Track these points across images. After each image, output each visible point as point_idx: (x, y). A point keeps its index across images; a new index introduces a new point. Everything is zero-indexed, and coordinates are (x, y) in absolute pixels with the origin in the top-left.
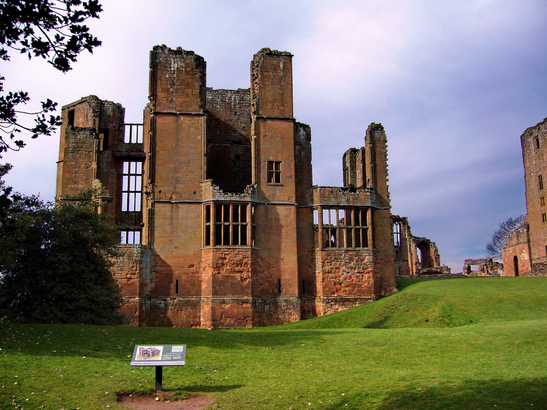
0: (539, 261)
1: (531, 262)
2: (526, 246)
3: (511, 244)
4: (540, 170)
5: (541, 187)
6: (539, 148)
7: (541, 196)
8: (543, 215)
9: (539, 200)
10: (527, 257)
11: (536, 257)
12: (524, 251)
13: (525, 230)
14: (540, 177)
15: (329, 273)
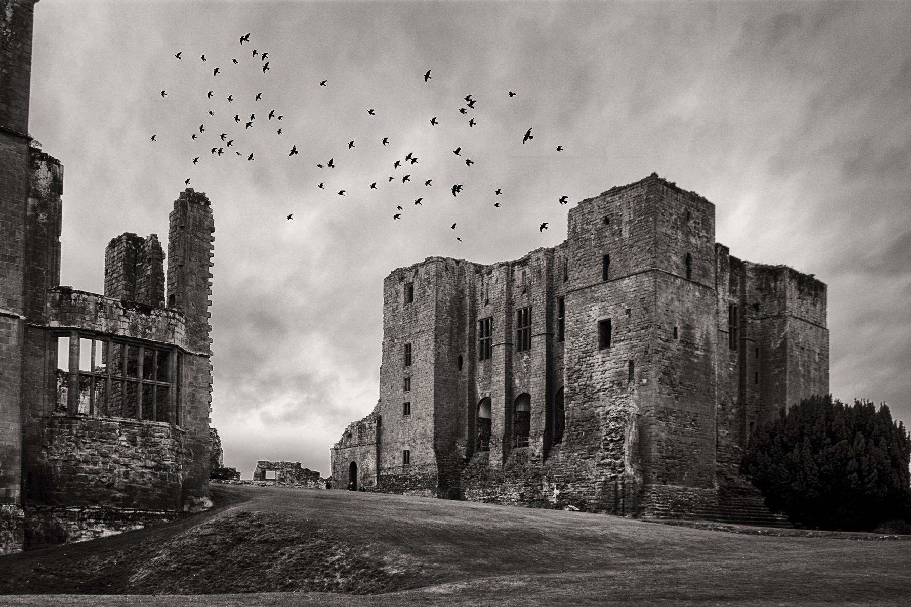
0: (390, 473)
1: (378, 473)
2: (373, 449)
3: (348, 444)
4: (409, 336)
5: (408, 361)
6: (411, 300)
7: (406, 376)
8: (405, 404)
9: (402, 382)
10: (372, 466)
11: (387, 466)
12: (369, 456)
13: (374, 425)
14: (408, 347)
15: (86, 462)
